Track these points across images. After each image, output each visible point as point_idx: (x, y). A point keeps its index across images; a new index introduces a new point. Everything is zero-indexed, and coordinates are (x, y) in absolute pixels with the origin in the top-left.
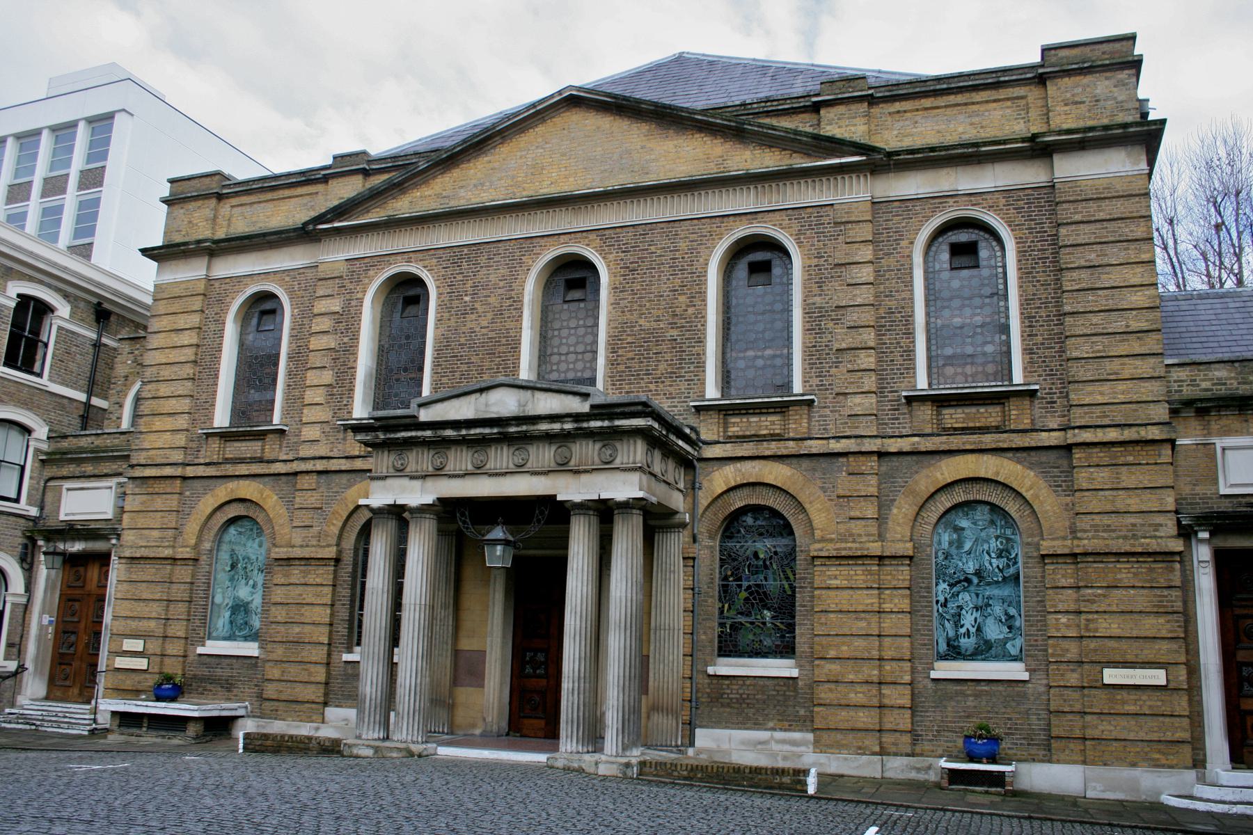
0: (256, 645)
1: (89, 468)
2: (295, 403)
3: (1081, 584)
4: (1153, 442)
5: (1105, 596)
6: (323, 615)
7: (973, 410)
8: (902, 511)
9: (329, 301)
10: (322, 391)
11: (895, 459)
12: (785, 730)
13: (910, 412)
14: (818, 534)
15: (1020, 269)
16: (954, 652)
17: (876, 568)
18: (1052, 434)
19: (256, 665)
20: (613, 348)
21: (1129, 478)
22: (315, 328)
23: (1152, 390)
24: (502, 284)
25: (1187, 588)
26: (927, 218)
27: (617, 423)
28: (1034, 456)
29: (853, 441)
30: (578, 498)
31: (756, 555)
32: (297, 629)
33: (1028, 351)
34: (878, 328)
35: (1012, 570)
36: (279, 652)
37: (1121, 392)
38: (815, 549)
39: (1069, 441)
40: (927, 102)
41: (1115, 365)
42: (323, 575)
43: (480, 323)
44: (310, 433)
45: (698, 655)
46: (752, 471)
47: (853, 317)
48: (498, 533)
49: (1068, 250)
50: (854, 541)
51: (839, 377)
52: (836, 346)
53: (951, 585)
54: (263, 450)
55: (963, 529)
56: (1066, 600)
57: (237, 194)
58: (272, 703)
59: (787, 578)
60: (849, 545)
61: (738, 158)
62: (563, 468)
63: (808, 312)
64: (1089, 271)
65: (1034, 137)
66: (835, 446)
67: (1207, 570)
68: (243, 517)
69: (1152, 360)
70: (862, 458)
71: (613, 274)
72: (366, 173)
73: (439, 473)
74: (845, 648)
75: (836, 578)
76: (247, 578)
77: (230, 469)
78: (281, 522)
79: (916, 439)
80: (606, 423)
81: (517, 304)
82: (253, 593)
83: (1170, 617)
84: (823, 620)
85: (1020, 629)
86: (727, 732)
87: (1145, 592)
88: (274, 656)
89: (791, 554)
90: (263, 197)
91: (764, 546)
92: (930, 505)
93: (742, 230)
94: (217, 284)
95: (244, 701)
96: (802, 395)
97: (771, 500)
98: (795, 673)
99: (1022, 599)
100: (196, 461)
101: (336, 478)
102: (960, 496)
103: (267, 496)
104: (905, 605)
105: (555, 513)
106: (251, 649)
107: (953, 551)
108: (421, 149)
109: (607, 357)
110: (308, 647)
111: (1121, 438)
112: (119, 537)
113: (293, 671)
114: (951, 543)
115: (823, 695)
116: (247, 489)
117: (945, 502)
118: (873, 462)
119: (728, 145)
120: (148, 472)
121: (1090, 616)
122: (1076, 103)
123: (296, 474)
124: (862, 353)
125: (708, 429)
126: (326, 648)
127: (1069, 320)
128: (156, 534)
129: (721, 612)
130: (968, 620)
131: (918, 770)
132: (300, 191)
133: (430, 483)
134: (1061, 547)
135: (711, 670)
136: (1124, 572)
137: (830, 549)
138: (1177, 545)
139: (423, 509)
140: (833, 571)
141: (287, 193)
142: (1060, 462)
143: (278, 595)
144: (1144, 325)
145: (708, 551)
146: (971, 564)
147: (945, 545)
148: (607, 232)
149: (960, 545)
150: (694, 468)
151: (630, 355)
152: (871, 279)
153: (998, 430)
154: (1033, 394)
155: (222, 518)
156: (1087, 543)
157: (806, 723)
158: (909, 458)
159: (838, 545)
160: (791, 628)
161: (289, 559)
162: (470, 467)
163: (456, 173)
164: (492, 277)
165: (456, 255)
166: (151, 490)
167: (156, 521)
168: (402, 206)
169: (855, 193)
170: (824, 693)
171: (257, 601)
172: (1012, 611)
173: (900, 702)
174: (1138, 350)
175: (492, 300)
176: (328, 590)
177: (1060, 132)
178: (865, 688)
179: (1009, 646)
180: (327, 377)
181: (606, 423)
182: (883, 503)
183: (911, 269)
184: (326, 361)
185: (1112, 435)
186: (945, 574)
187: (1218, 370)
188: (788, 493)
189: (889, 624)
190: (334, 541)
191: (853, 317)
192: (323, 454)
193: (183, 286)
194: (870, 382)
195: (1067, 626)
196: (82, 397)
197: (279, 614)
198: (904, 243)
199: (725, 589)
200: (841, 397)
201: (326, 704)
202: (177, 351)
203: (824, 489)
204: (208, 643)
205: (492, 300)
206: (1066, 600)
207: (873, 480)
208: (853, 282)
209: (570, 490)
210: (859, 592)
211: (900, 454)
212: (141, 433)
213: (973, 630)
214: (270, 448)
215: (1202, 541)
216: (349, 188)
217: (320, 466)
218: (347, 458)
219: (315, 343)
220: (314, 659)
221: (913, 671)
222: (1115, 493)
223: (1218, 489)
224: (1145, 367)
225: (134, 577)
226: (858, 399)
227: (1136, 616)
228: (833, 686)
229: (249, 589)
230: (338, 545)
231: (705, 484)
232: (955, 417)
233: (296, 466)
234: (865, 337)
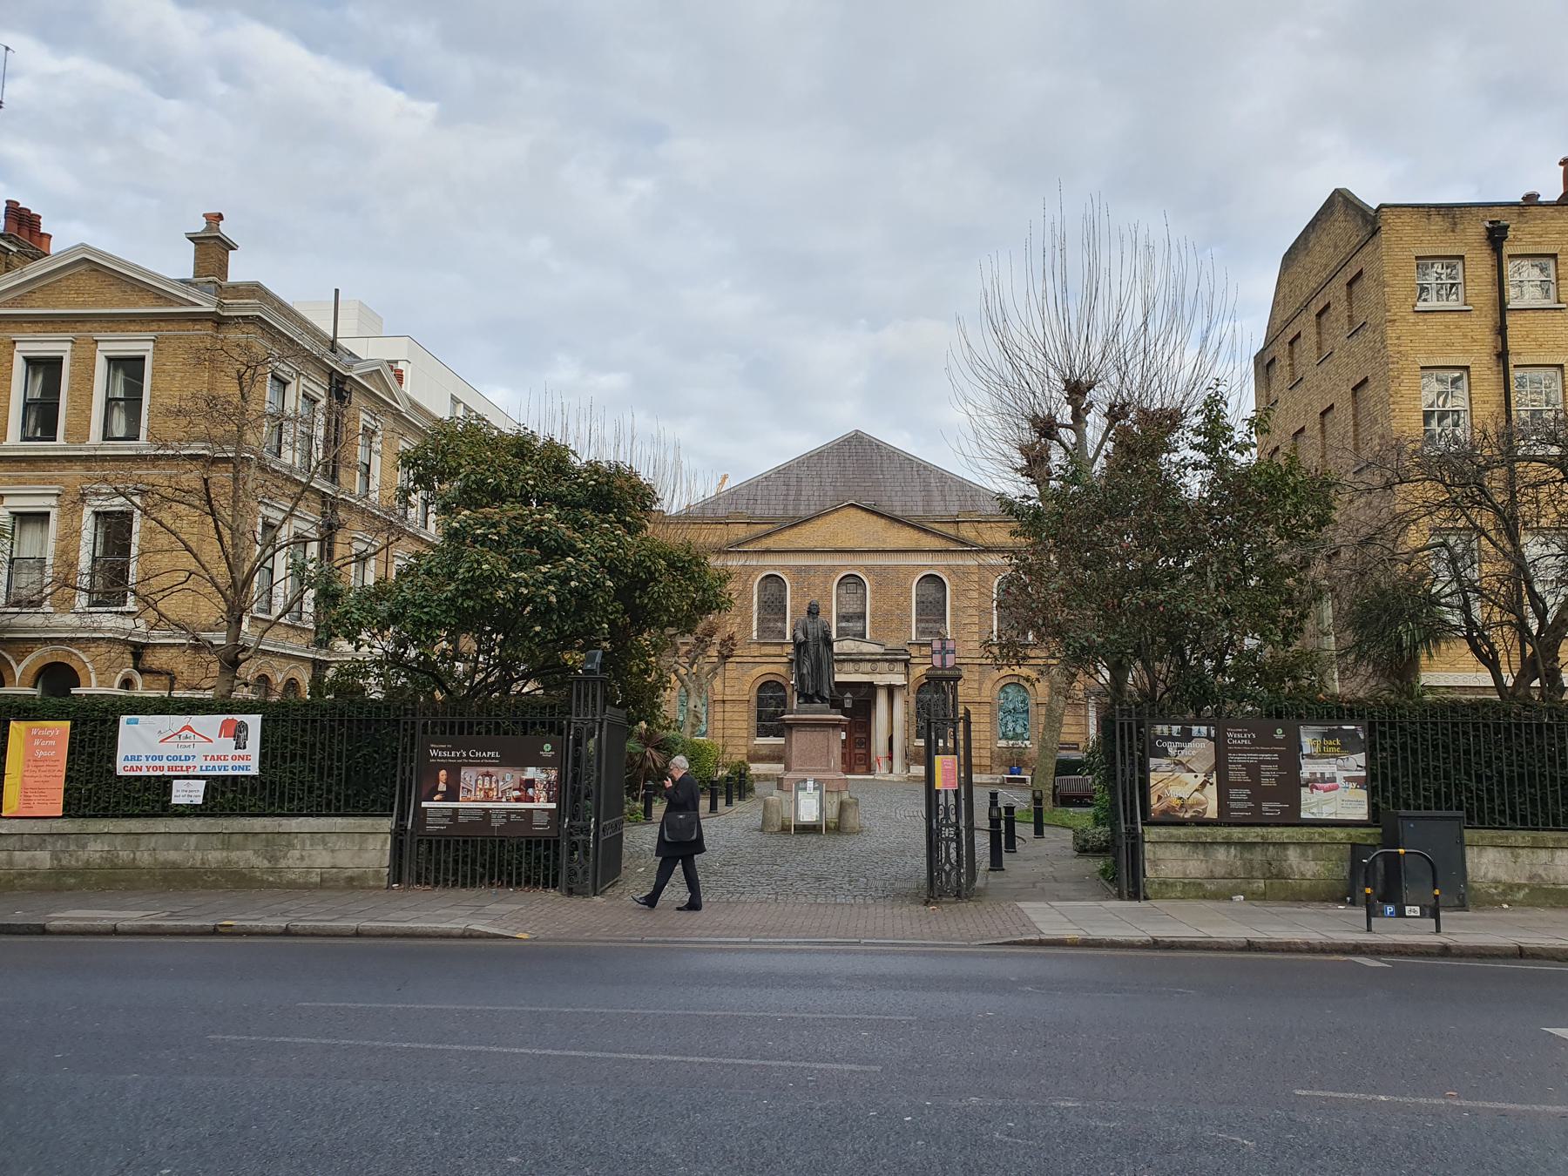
8: (988, 685)
20: (872, 616)
62: (873, 672)
117: (1003, 682)
125: (914, 651)
130: (1010, 725)
145: (912, 698)
165: (799, 570)
168: (769, 543)
169: (971, 561)
191: (970, 611)
194: (976, 637)
209: (878, 679)
216: (741, 532)
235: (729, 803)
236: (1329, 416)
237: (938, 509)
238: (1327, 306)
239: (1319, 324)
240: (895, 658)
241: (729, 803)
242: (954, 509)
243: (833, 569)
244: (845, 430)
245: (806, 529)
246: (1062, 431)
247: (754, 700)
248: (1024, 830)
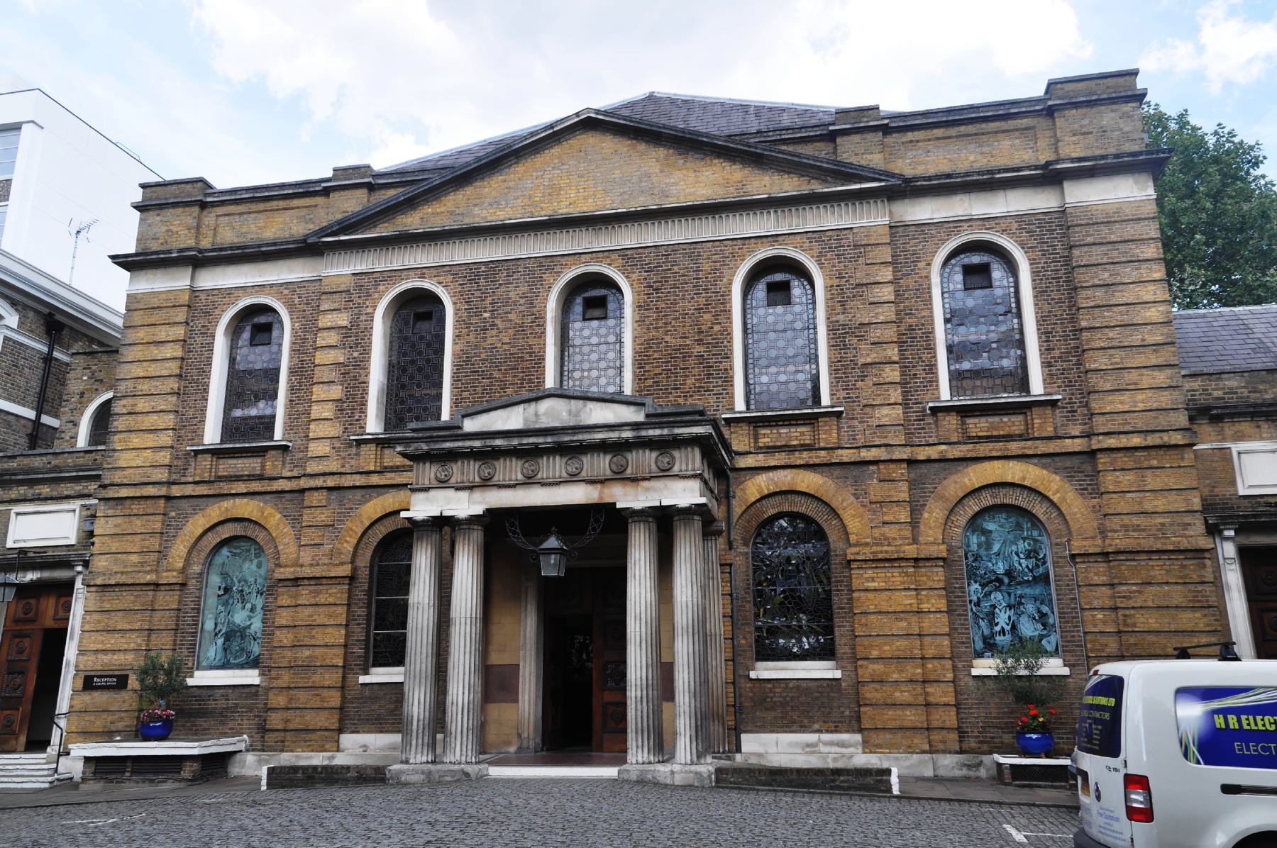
0: (256, 672)
1: (45, 490)
2: (299, 417)
3: (1116, 581)
4: (1176, 446)
5: (1139, 592)
6: (338, 636)
7: (997, 419)
8: (934, 514)
9: (335, 315)
10: (330, 405)
11: (923, 466)
12: (832, 732)
13: (936, 422)
14: (853, 538)
15: (1034, 288)
16: (990, 647)
17: (911, 570)
18: (1076, 441)
19: (256, 694)
20: (639, 363)
21: (1153, 481)
22: (320, 342)
23: (1165, 399)
24: (522, 301)
25: (1218, 584)
26: (944, 241)
27: (677, 431)
28: (1059, 462)
29: (883, 449)
30: (638, 505)
31: (788, 559)
32: (307, 653)
33: (1047, 364)
34: (900, 344)
35: (1041, 570)
36: (285, 678)
37: (1141, 400)
38: (851, 553)
39: (1094, 447)
40: (939, 132)
41: (1134, 376)
42: (337, 594)
43: (500, 339)
44: (316, 449)
45: (740, 660)
46: (785, 479)
47: (875, 334)
48: (552, 542)
49: (1081, 270)
50: (889, 545)
51: (866, 390)
52: (861, 361)
53: (983, 586)
54: (263, 467)
55: (991, 532)
56: (1102, 596)
57: (223, 203)
58: (277, 734)
59: (821, 582)
60: (885, 548)
61: (756, 184)
62: (619, 476)
63: (833, 328)
64: (1103, 289)
65: (1048, 163)
66: (866, 455)
67: (1233, 567)
68: (240, 539)
69: (1169, 371)
70: (892, 466)
71: (636, 293)
72: (371, 187)
73: (486, 483)
74: (887, 648)
75: (873, 580)
76: (244, 601)
77: (225, 488)
78: (286, 541)
79: (944, 447)
80: (666, 432)
81: (539, 320)
82: (250, 618)
83: (1206, 611)
84: (863, 620)
85: (1053, 625)
86: (774, 736)
87: (1179, 587)
88: (280, 683)
89: (826, 557)
90: (254, 207)
92: (959, 510)
94: (203, 296)
95: (241, 734)
96: (832, 407)
97: (804, 507)
98: (838, 674)
99: (1054, 597)
100: (183, 480)
101: (349, 494)
102: (987, 500)
103: (272, 516)
104: (942, 605)
105: (608, 524)
106: (251, 677)
107: (983, 552)
108: (429, 165)
109: (634, 372)
110: (320, 670)
111: (1144, 444)
112: (86, 564)
113: (303, 697)
114: (979, 545)
115: (868, 695)
116: (246, 508)
117: (973, 506)
118: (902, 470)
119: (747, 171)
120: (124, 492)
121: (1127, 612)
122: (1084, 134)
123: (303, 491)
124: (887, 368)
125: (739, 440)
126: (341, 671)
127: (1085, 335)
128: (135, 558)
129: (757, 615)
130: (1003, 618)
131: (969, 767)
132: (296, 202)
133: (477, 495)
134: (1094, 546)
135: (753, 675)
136: (1157, 569)
137: (866, 553)
138: (1204, 542)
139: (473, 520)
140: (870, 573)
141: (282, 204)
142: (1084, 467)
143: (283, 617)
144: (1158, 339)
145: (741, 557)
146: (1000, 564)
147: (974, 547)
148: (629, 252)
149: (989, 546)
150: (727, 478)
151: (658, 371)
152: (892, 298)
153: (1021, 437)
154: (1053, 404)
155: (213, 539)
156: (1119, 541)
157: (855, 724)
158: (936, 465)
159: (875, 548)
160: (829, 630)
161: (297, 579)
162: (520, 477)
163: (469, 190)
164: (512, 295)
165: (472, 274)
166: (127, 512)
167: (135, 544)
168: (413, 221)
170: (870, 693)
171: (257, 625)
172: (1045, 609)
173: (945, 700)
174: (1154, 362)
175: (512, 316)
176: (342, 611)
177: (1073, 160)
178: (910, 687)
179: (1044, 642)
180: (336, 392)
181: (666, 432)
182: (916, 510)
183: (930, 288)
184: (333, 376)
185: (1136, 441)
186: (975, 575)
187: (1229, 379)
188: (819, 499)
189: (928, 624)
190: (349, 559)
191: (875, 334)
192: (335, 470)
193: (164, 296)
194: (896, 395)
195: (1104, 622)
196: (31, 414)
197: (284, 637)
198: (921, 265)
199: (760, 594)
200: (868, 410)
201: (341, 730)
202: (159, 364)
203: (856, 496)
204: (197, 673)
205: (512, 316)
206: (1102, 596)
207: (904, 487)
208: (875, 300)
209: (628, 498)
210: (897, 593)
211: (929, 461)
212: (114, 450)
213: (1008, 628)
214: (272, 465)
215: (1228, 538)
216: (353, 203)
217: (331, 482)
218: (361, 473)
219: (320, 357)
220: (327, 683)
221: (955, 668)
222: (1141, 495)
223: (1236, 490)
224: (1161, 377)
225: (107, 606)
226: (885, 411)
227: (1172, 611)
228: (877, 686)
229: (246, 613)
230: (352, 562)
231: (739, 493)
232: (978, 426)
233: (304, 483)
234: (889, 352)
243: (551, 263)
245: (491, 187)
247: (364, 574)
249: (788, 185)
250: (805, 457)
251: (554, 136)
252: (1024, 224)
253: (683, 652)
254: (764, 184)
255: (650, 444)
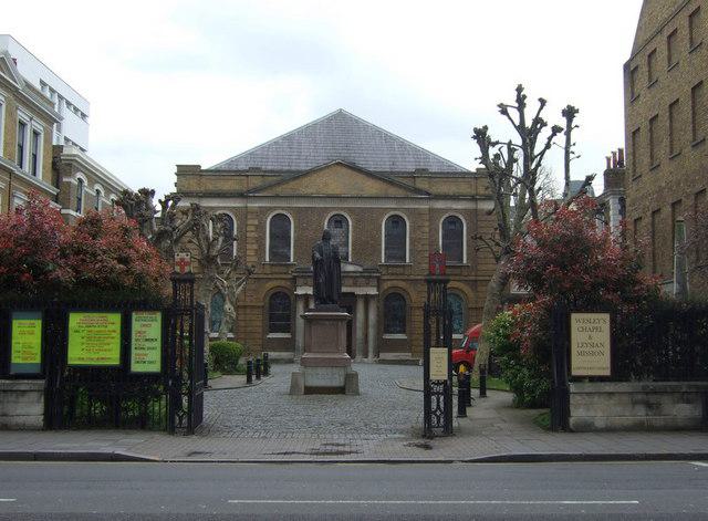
62: (355, 285)
91: (396, 304)
93: (392, 213)
153: (460, 275)
160: (405, 325)
169: (424, 206)
180: (255, 247)
194: (427, 260)
209: (359, 291)
216: (256, 182)
219: (248, 235)
235: (258, 378)
236: (676, 107)
237: (400, 167)
238: (676, 31)
239: (669, 44)
240: (367, 276)
241: (258, 378)
242: (411, 168)
243: (326, 210)
244: (333, 109)
245: (305, 181)
246: (509, 110)
247: (267, 305)
248: (475, 392)
249: (400, 193)
250: (401, 277)
251: (327, 167)
252: (465, 212)
253: (371, 332)
254: (392, 191)
255: (364, 277)
